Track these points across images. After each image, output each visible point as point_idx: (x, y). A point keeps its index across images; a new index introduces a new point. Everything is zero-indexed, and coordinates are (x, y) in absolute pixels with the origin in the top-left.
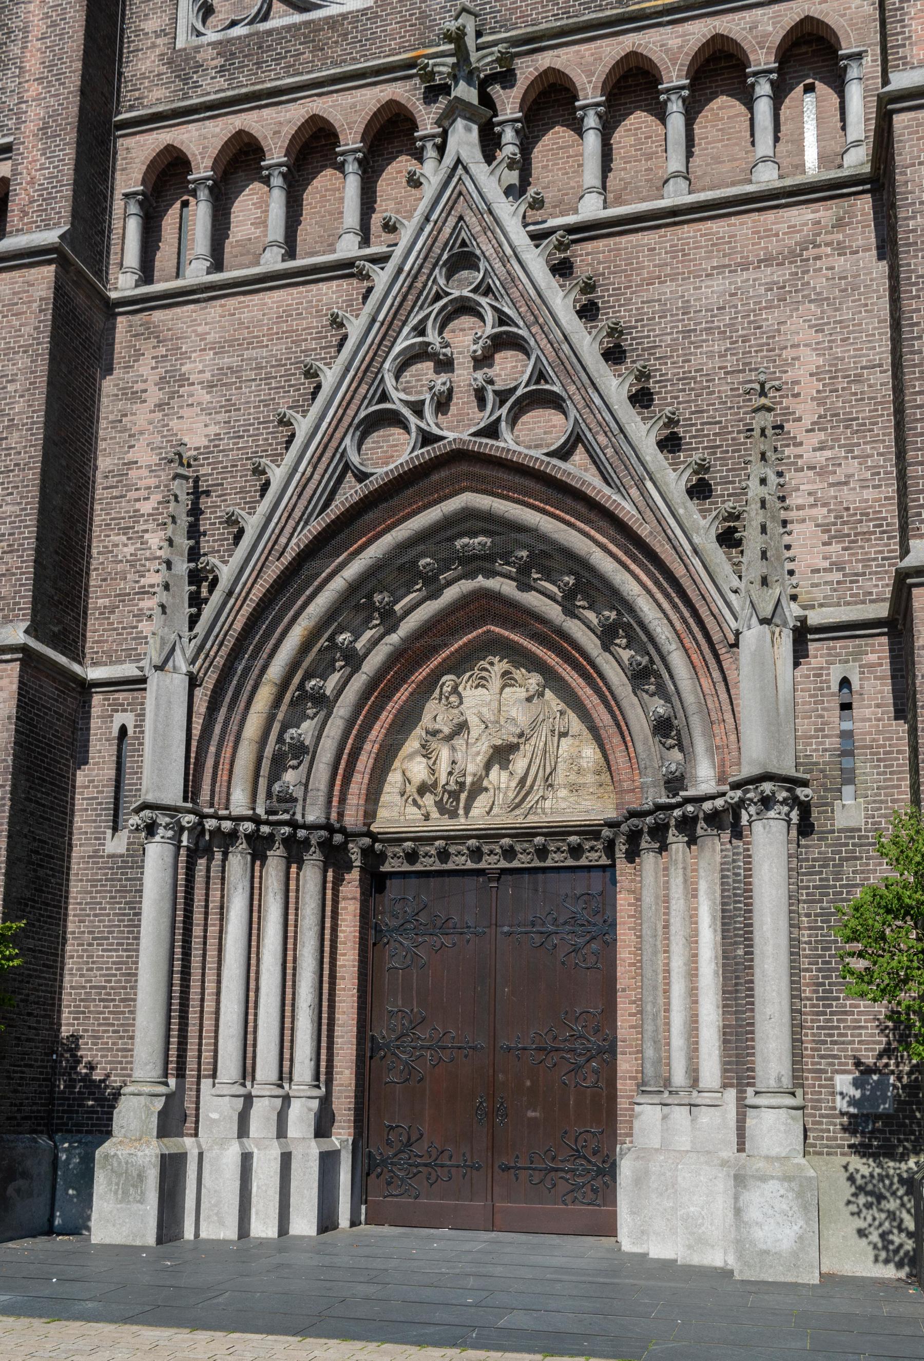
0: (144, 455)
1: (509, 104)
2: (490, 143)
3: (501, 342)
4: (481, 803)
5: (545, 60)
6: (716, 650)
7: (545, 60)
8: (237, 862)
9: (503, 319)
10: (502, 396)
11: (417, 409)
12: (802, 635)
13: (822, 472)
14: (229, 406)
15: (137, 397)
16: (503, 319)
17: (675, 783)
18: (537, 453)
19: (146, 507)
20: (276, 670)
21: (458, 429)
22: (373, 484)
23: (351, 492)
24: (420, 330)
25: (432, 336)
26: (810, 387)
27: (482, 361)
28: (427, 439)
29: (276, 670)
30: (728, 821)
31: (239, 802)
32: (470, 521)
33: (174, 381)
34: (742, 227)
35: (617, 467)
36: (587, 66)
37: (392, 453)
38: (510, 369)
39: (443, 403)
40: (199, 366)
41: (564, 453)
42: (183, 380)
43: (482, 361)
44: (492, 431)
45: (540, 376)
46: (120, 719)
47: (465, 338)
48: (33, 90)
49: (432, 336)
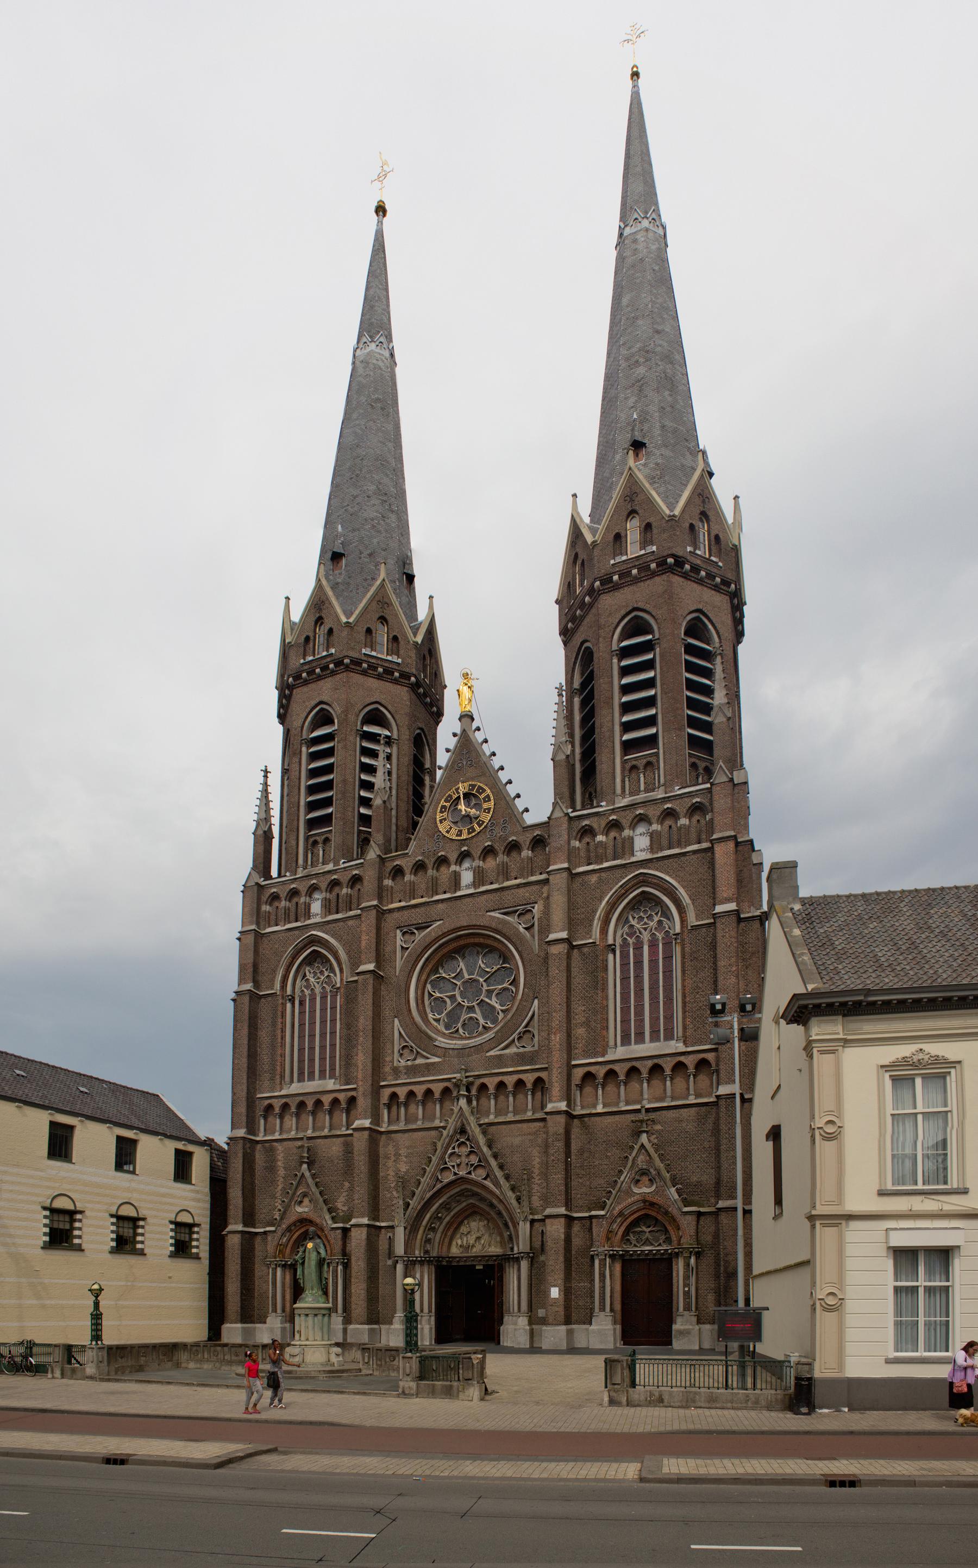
0: (392, 1174)
1: (474, 1091)
2: (469, 1101)
3: (471, 1152)
4: (474, 1250)
5: (482, 1080)
6: (516, 1225)
7: (482, 1080)
8: (418, 1267)
9: (472, 1147)
10: (472, 1165)
11: (453, 1166)
12: (533, 1222)
13: (539, 1185)
14: (411, 1162)
15: (389, 1158)
16: (472, 1147)
17: (512, 1249)
18: (479, 1179)
19: (392, 1185)
20: (424, 1223)
21: (462, 1173)
22: (443, 1184)
23: (439, 1186)
24: (454, 1148)
25: (456, 1150)
26: (537, 1166)
27: (468, 1155)
28: (455, 1174)
29: (424, 1223)
30: (517, 1260)
31: (417, 1253)
32: (467, 1190)
33: (397, 1155)
34: (525, 1125)
35: (497, 1184)
36: (491, 1083)
37: (448, 1178)
38: (474, 1160)
39: (458, 1165)
40: (403, 1152)
41: (485, 1179)
42: (400, 1155)
43: (468, 1155)
44: (470, 1173)
45: (480, 1161)
46: (389, 1234)
47: (464, 1150)
48: (360, 1083)
49: (456, 1150)
